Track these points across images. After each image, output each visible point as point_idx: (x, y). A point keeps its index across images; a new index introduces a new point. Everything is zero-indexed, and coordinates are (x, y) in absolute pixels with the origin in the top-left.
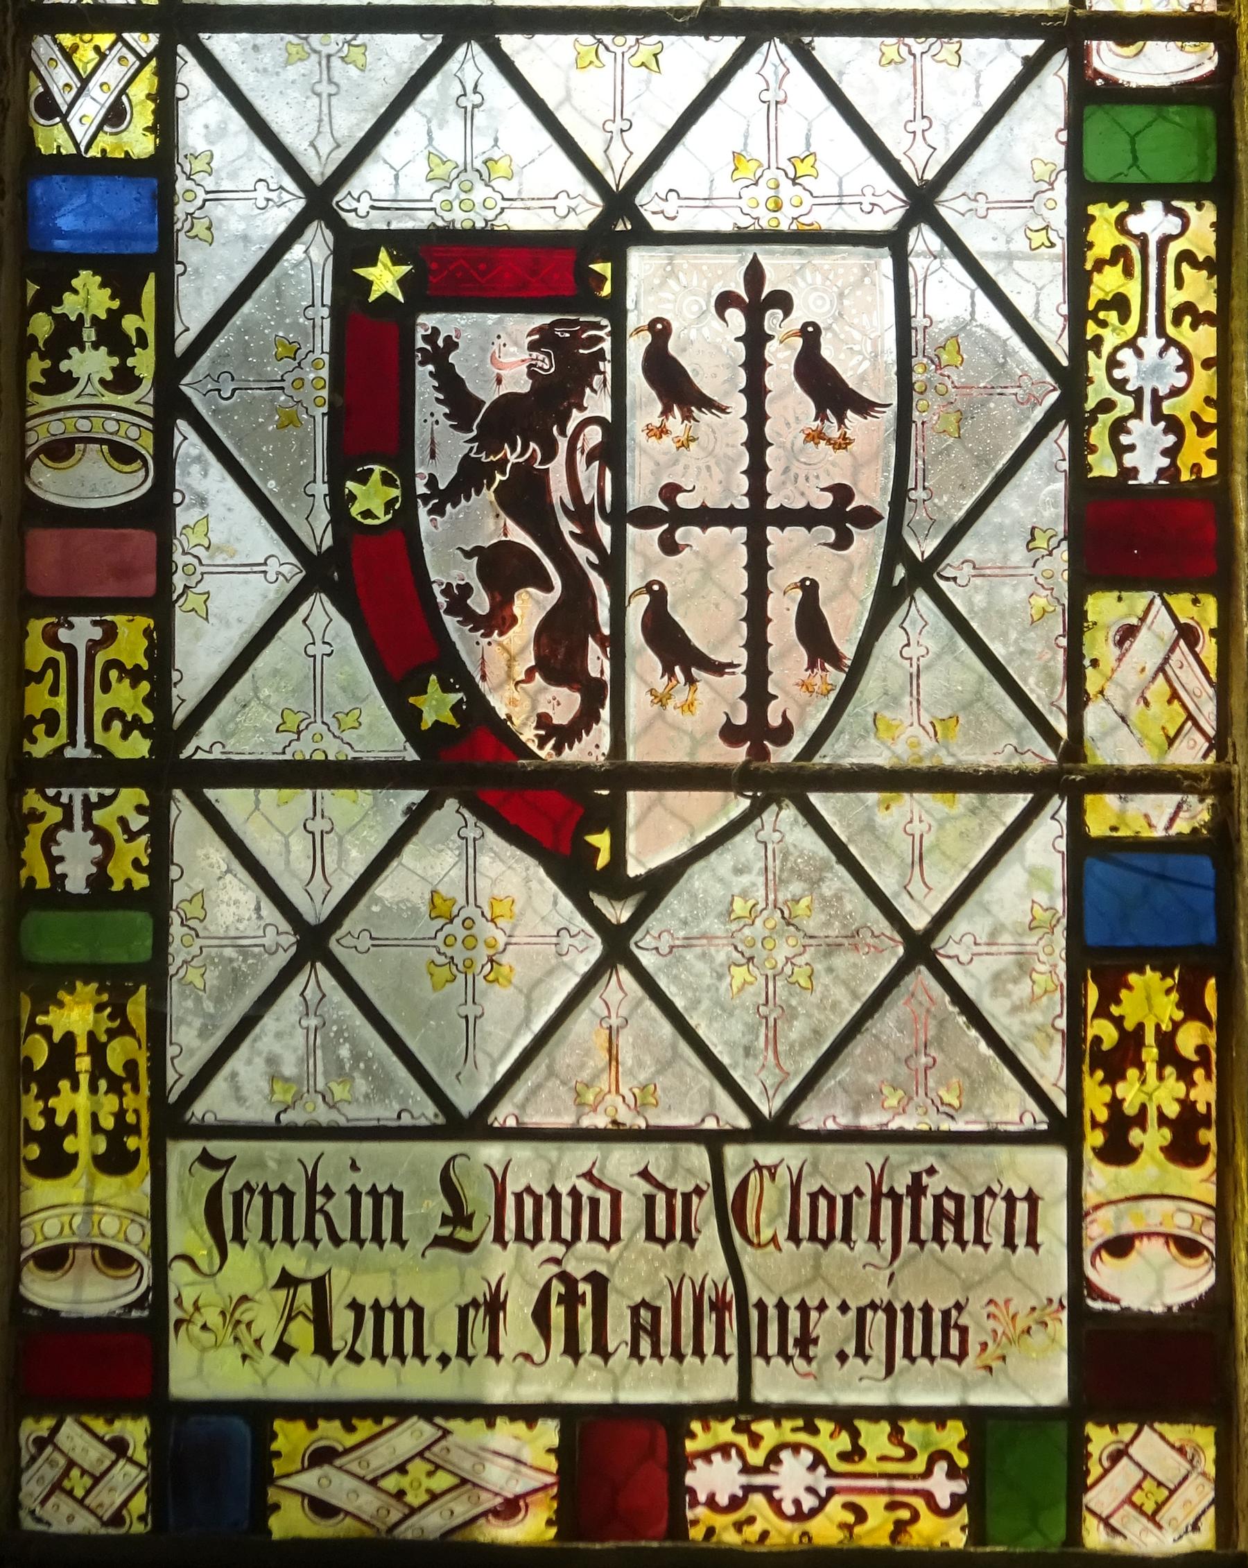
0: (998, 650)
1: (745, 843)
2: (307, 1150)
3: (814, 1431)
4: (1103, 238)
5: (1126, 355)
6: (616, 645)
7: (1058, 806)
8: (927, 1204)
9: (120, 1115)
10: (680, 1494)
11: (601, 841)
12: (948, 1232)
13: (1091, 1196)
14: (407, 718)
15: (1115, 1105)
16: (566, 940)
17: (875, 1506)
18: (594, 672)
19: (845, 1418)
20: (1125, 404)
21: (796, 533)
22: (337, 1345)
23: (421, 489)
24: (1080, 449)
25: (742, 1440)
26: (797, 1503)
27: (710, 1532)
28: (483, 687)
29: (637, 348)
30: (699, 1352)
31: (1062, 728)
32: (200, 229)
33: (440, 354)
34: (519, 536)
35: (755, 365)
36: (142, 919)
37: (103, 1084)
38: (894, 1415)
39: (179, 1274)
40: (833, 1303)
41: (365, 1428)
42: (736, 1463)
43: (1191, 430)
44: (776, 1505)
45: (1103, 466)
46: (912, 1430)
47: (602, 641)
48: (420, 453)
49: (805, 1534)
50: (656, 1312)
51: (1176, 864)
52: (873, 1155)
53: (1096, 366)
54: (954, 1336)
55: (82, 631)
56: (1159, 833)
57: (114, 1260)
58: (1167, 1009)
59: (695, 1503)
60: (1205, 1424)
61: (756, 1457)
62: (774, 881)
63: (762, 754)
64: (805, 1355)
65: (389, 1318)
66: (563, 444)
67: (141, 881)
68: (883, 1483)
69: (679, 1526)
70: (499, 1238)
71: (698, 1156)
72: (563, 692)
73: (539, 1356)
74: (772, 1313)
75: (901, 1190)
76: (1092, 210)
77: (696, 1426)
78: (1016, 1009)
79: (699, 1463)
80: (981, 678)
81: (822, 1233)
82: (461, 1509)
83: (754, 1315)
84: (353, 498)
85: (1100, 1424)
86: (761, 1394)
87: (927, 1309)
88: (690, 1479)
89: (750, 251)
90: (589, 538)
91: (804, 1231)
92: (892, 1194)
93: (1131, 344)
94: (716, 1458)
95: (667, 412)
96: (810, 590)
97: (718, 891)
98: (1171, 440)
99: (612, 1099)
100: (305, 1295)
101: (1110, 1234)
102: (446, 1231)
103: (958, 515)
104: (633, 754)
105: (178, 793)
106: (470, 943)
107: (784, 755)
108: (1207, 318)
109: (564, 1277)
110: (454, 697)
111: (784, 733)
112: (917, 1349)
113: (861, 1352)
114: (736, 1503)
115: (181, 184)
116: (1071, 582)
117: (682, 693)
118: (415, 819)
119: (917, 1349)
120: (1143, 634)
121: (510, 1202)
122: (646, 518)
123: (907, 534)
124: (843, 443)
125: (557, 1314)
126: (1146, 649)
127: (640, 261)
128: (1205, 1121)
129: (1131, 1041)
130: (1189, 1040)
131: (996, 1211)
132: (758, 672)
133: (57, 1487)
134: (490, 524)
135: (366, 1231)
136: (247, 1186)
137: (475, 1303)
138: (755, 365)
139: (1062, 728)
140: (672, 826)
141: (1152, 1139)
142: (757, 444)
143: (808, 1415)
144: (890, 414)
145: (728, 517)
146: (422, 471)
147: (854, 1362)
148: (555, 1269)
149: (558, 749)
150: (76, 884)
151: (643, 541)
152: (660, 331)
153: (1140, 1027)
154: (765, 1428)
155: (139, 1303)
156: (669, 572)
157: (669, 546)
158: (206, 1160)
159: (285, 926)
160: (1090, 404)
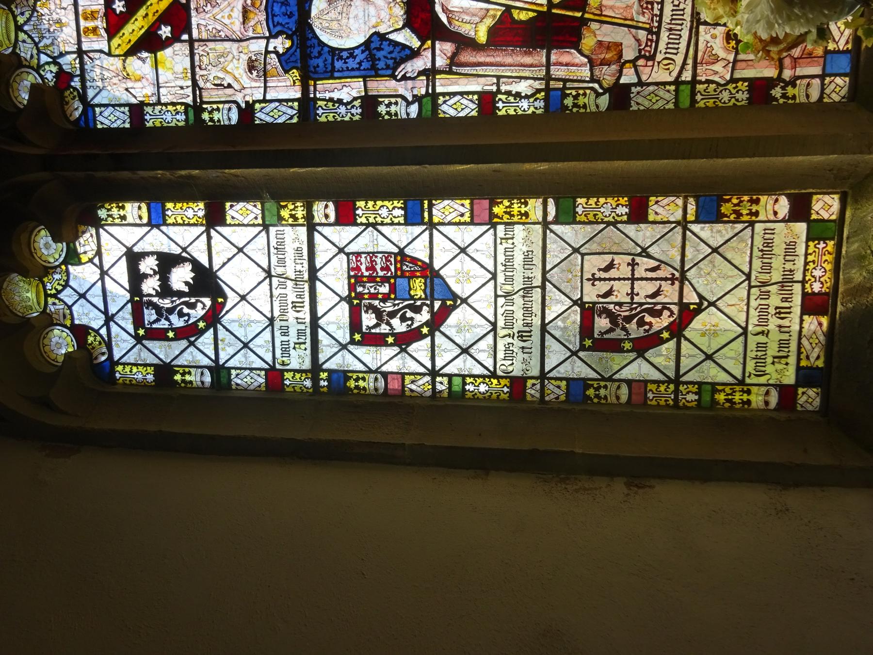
0: (659, 237)
1: (693, 282)
2: (748, 359)
3: (808, 269)
4: (583, 218)
5: (604, 214)
6: (656, 304)
7: (690, 226)
8: (765, 249)
9: (740, 391)
10: (820, 293)
11: (692, 307)
12: (771, 245)
13: (766, 219)
14: (668, 340)
15: (747, 214)
16: (710, 313)
17: (824, 258)
18: (660, 308)
19: (806, 263)
20: (613, 214)
21: (636, 272)
22: (786, 355)
23: (626, 337)
24: (621, 222)
25: (809, 282)
26: (823, 272)
27: (827, 288)
28: (662, 327)
29: (601, 300)
30: (791, 290)
31: (674, 225)
32: (578, 373)
33: (602, 334)
34: (635, 320)
35: (605, 279)
36: (704, 386)
37: (734, 394)
38: (806, 255)
39: (771, 382)
40: (783, 266)
41: (803, 350)
42: (814, 283)
43: (618, 202)
44: (823, 276)
45: (625, 218)
46: (810, 251)
47: (655, 306)
48: (619, 337)
49: (829, 271)
50: (783, 298)
51: (700, 204)
52: (754, 260)
53: (606, 219)
54: (791, 244)
55: (650, 395)
56: (695, 207)
57: (767, 393)
58: (729, 205)
59: (821, 291)
60: (812, 197)
61: (813, 280)
62: (701, 276)
63: (677, 278)
64: (793, 271)
65: (781, 345)
66: (619, 313)
67: (696, 386)
68: (820, 257)
69: (826, 294)
70: (767, 326)
71: (753, 290)
72: (664, 313)
73: (790, 319)
74: (785, 277)
75: (762, 254)
76: (578, 220)
77: (806, 291)
78: (728, 233)
79: (813, 290)
80: (665, 240)
81: (769, 268)
82: (820, 332)
83: (785, 280)
84: (627, 349)
85: (811, 217)
86: (800, 279)
87: (786, 249)
88: (816, 292)
89: (584, 281)
90: (636, 308)
91: (768, 271)
92: (762, 255)
93: (602, 213)
94: (813, 287)
95: (613, 295)
96: (646, 270)
97: (702, 287)
98: (620, 206)
99: (741, 305)
100: (776, 360)
101: (773, 215)
102: (765, 335)
103: (633, 244)
104: (676, 301)
105: (681, 380)
106: (710, 330)
107: (677, 275)
108: (598, 200)
109: (775, 314)
110: (664, 332)
111: (673, 275)
112: (793, 251)
113: (793, 261)
114: (822, 283)
115: (571, 376)
116: (646, 223)
117: (665, 292)
118: (686, 339)
119: (793, 251)
120: (657, 210)
121: (760, 324)
122: (632, 299)
123: (637, 253)
124: (619, 264)
125: (782, 315)
126: (660, 210)
127: (585, 299)
128: (751, 198)
129: (735, 212)
130: (735, 201)
131: (767, 236)
132: (661, 279)
133: (811, 404)
134: (633, 326)
135: (764, 349)
136: (755, 370)
137: (779, 330)
138: (605, 279)
139: (674, 225)
140: (690, 294)
141: (754, 208)
142: (619, 279)
143: (805, 270)
144: (615, 257)
145: (633, 284)
146: (623, 337)
147: (795, 262)
148: (774, 316)
149: (674, 314)
150: (697, 397)
151: (636, 299)
152: (599, 296)
153: (732, 210)
154: (807, 278)
155: (776, 389)
156: (643, 294)
157: (638, 294)
158: (749, 377)
159: (706, 362)
160: (613, 220)
